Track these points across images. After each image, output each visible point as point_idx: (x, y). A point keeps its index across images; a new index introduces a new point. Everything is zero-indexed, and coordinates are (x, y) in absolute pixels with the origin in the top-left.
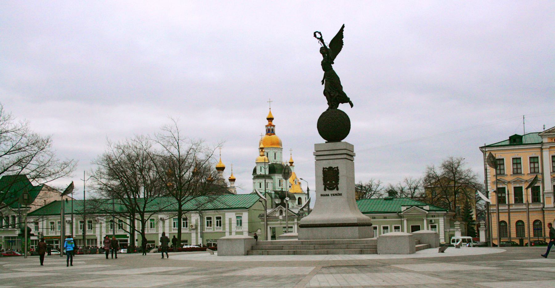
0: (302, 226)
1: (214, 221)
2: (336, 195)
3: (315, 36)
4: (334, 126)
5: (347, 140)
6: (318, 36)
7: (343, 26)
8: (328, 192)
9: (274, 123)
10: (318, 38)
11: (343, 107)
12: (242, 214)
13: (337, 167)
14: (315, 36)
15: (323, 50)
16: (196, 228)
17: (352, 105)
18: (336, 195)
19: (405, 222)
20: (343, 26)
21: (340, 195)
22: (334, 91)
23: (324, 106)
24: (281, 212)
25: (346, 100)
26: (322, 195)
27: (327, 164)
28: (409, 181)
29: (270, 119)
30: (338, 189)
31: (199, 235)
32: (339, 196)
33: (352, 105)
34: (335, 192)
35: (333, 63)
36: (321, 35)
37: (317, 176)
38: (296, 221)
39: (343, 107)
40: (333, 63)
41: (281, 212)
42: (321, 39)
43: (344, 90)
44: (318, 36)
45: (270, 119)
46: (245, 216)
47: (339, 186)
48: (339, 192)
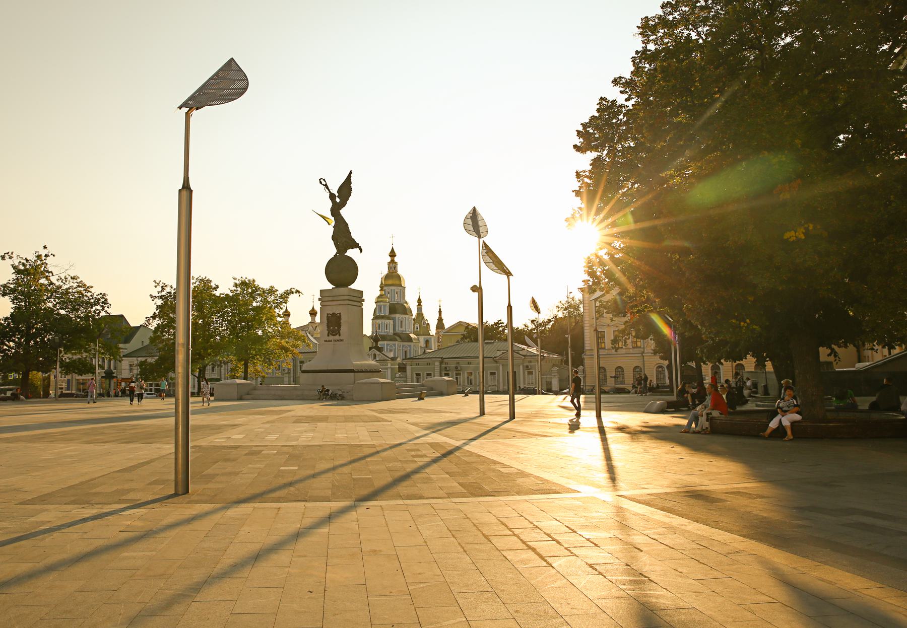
4: (341, 271)
5: (353, 286)
7: (351, 172)
8: (331, 338)
9: (396, 259)
11: (351, 253)
15: (332, 197)
16: (289, 373)
17: (361, 251)
19: (501, 367)
20: (351, 172)
22: (343, 237)
23: (332, 251)
24: (375, 356)
25: (355, 245)
29: (393, 254)
33: (361, 251)
34: (337, 337)
38: (389, 365)
39: (351, 253)
41: (375, 356)
42: (326, 185)
43: (353, 236)
44: (323, 183)
45: (393, 254)
48: (341, 338)
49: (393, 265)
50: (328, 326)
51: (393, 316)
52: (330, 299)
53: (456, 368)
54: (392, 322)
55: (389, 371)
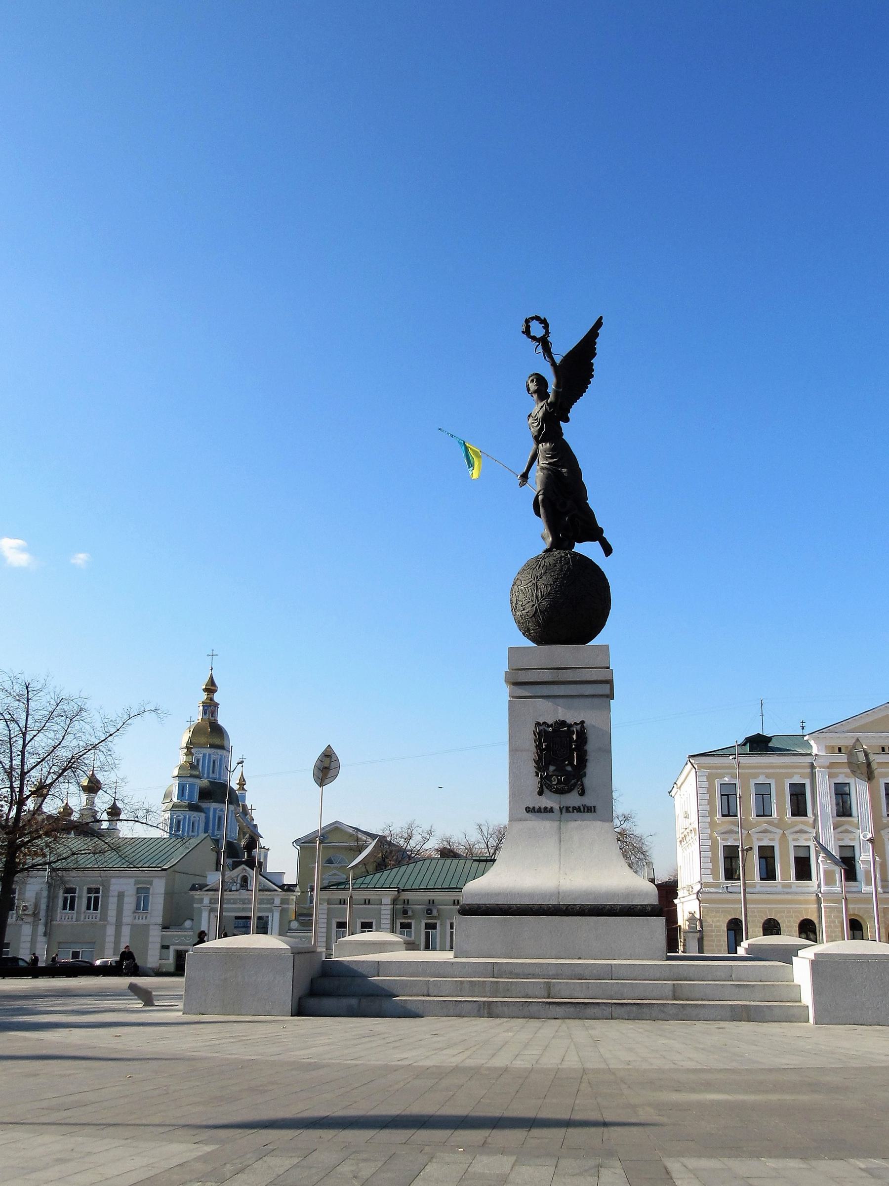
0: (470, 910)
1: (80, 897)
2: (578, 810)
3: (527, 332)
6: (537, 330)
7: (599, 324)
9: (217, 697)
10: (534, 338)
11: (588, 549)
12: (151, 883)
13: (582, 722)
14: (527, 332)
16: (35, 915)
18: (578, 810)
20: (599, 324)
21: (590, 810)
22: (566, 506)
26: (528, 810)
27: (551, 712)
28: (484, 829)
29: (211, 688)
30: (582, 793)
31: (41, 929)
32: (587, 815)
33: (608, 550)
34: (573, 799)
35: (567, 420)
36: (546, 326)
37: (514, 751)
39: (588, 549)
40: (567, 420)
42: (544, 343)
43: (591, 502)
45: (211, 688)
46: (159, 887)
47: (586, 781)
48: (587, 801)
49: (210, 707)
50: (542, 764)
51: (204, 805)
52: (546, 676)
53: (429, 912)
54: (203, 815)
55: (277, 915)
